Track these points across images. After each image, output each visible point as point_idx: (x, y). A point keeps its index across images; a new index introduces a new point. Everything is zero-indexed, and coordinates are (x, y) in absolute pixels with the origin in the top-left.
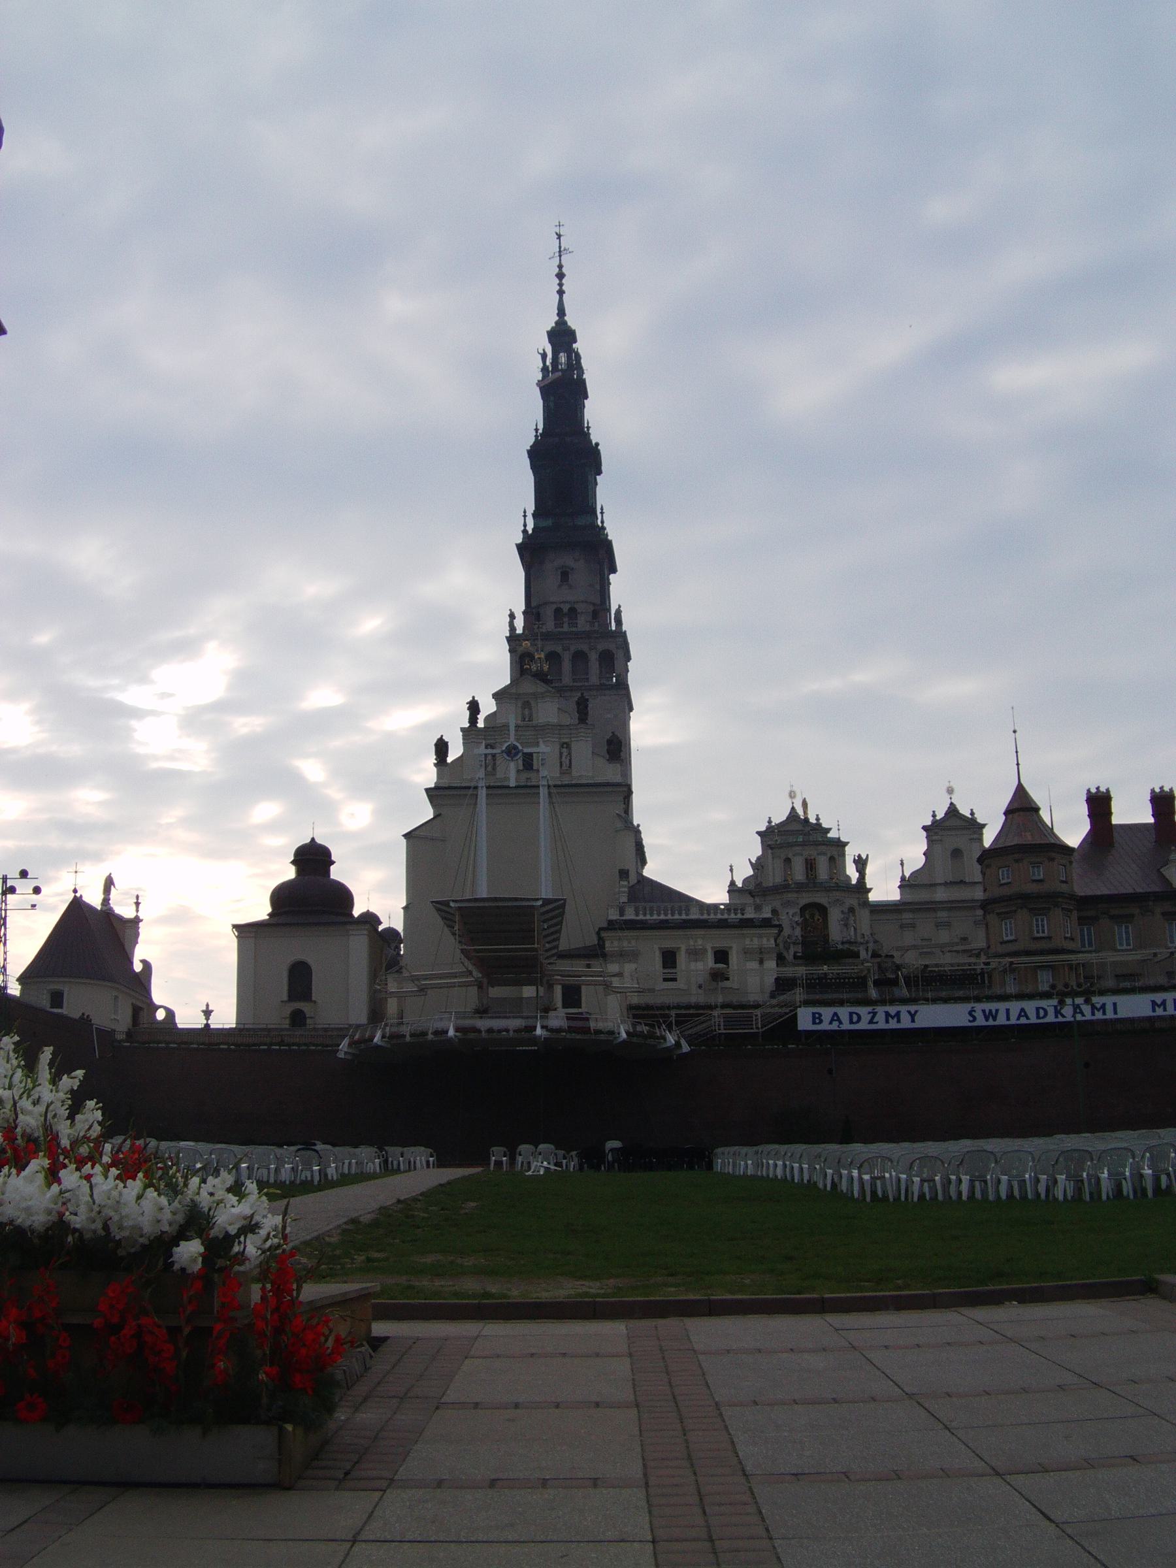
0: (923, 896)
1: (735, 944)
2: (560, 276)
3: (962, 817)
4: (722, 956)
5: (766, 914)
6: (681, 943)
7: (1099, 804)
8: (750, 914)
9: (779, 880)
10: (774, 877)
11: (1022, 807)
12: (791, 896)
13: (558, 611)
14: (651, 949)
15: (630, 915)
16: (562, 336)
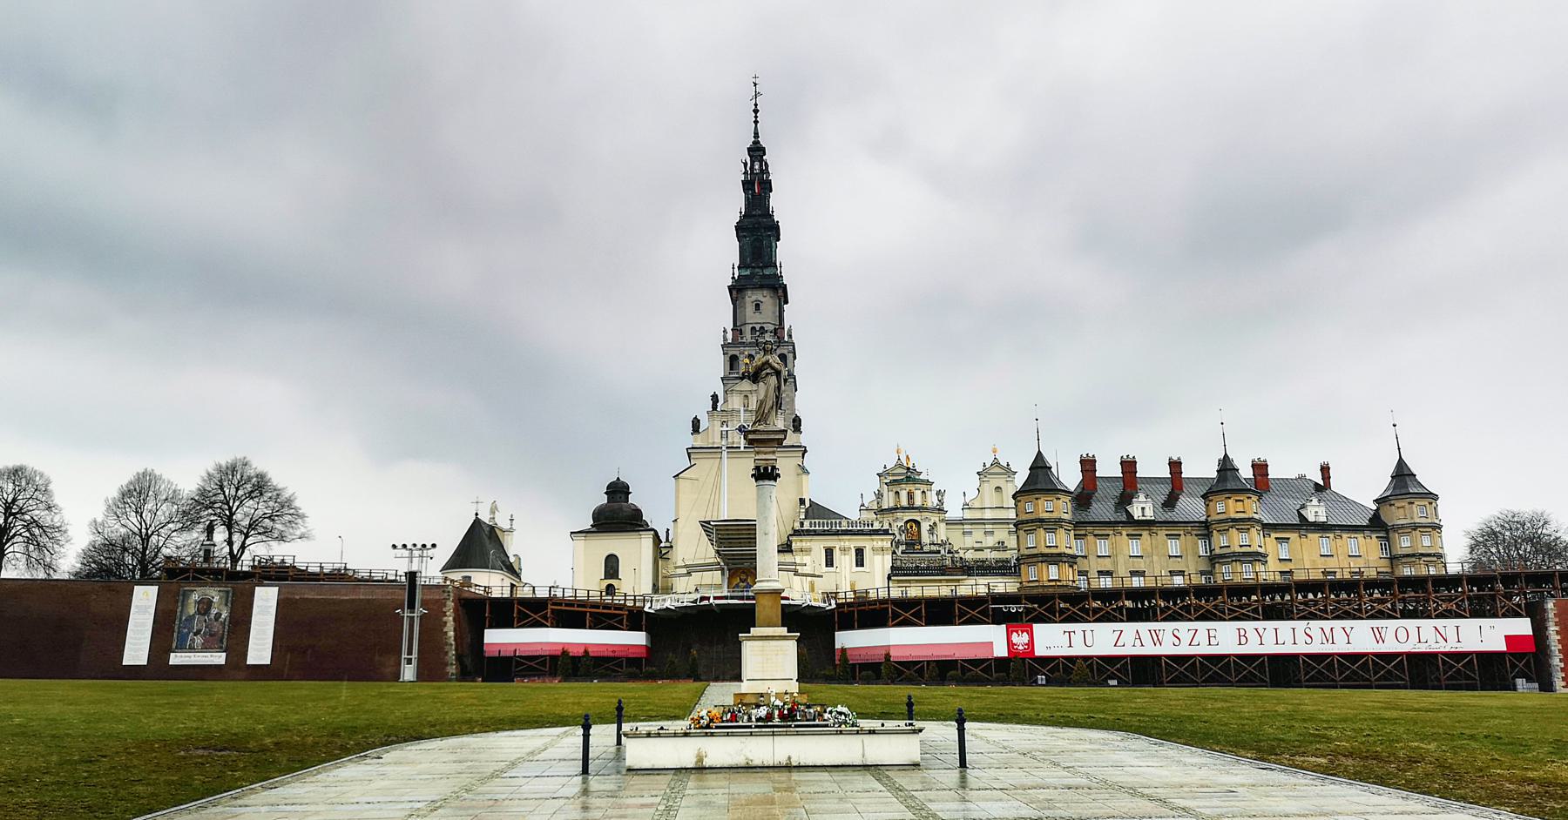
0: (977, 515)
1: (867, 543)
2: (756, 111)
3: (1001, 467)
4: (860, 552)
5: (886, 527)
6: (835, 543)
7: (1088, 465)
8: (877, 526)
9: (892, 505)
10: (889, 501)
11: (1040, 467)
12: (899, 515)
13: (753, 329)
14: (818, 546)
15: (807, 526)
16: (757, 151)
